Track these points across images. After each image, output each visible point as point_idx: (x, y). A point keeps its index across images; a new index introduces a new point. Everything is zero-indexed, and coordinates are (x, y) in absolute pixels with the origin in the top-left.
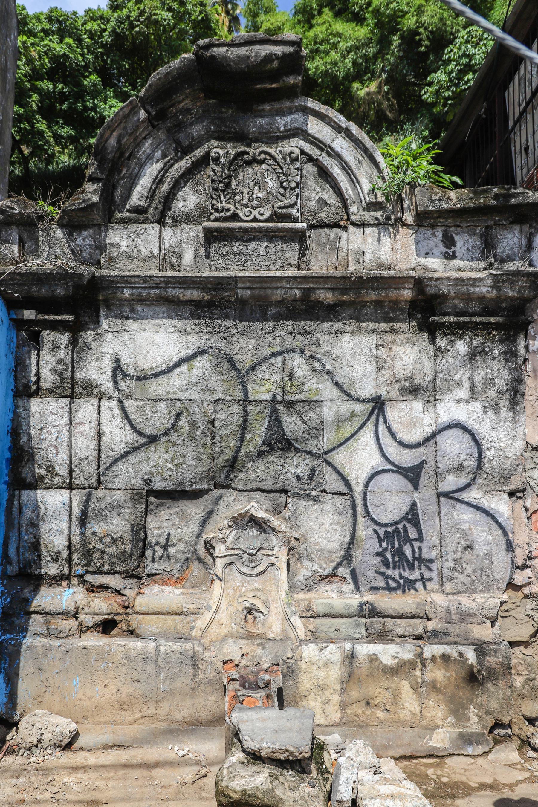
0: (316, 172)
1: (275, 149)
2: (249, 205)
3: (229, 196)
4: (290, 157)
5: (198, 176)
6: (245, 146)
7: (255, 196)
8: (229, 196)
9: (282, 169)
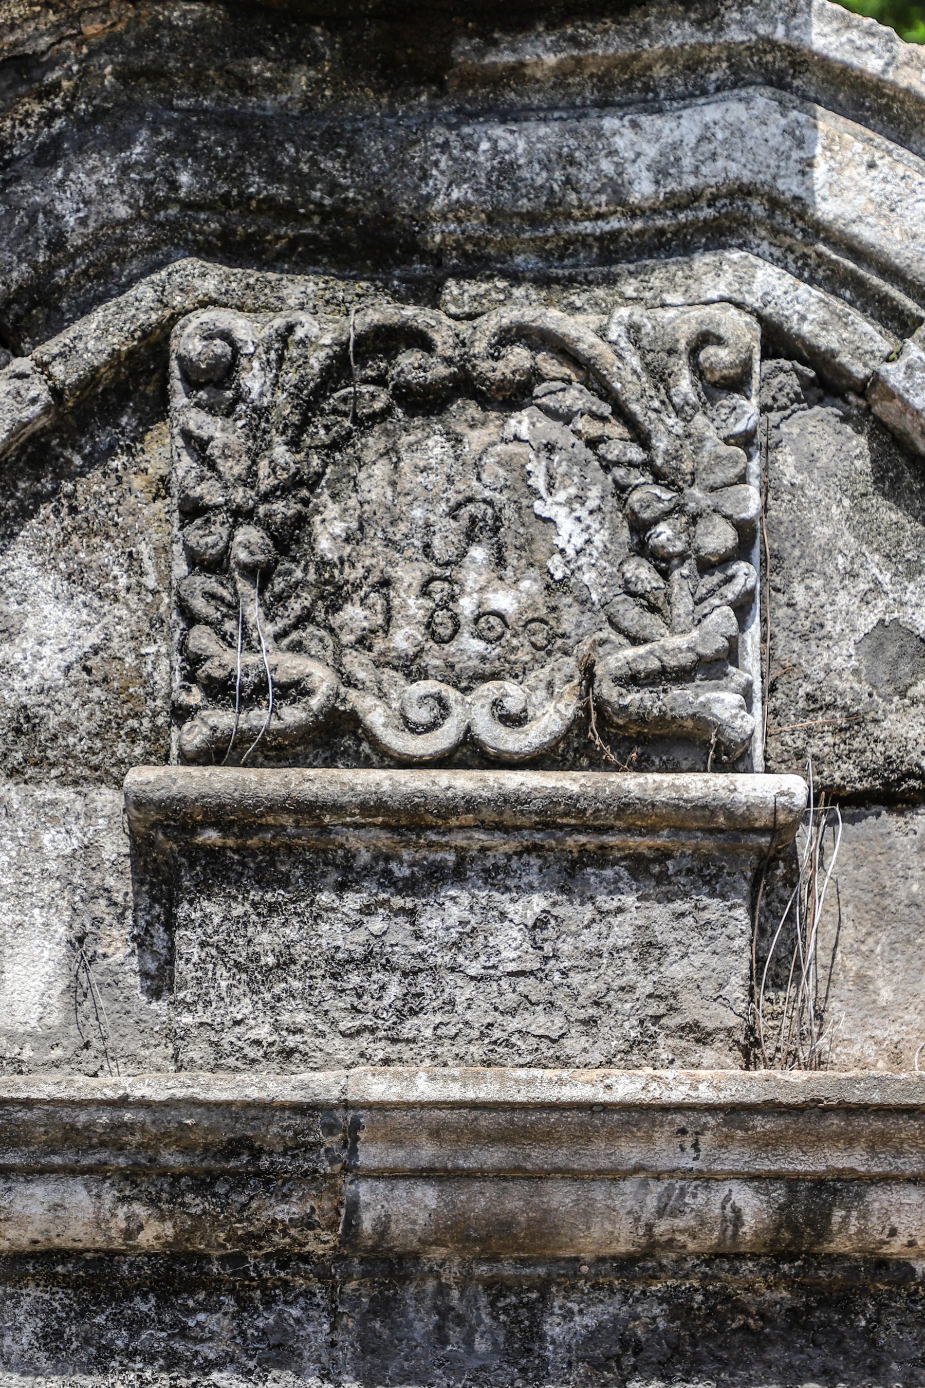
0: (864, 465)
1: (594, 319)
2: (432, 660)
3: (296, 606)
4: (698, 370)
5: (95, 481)
6: (401, 299)
7: (466, 606)
8: (296, 606)
9: (642, 438)
